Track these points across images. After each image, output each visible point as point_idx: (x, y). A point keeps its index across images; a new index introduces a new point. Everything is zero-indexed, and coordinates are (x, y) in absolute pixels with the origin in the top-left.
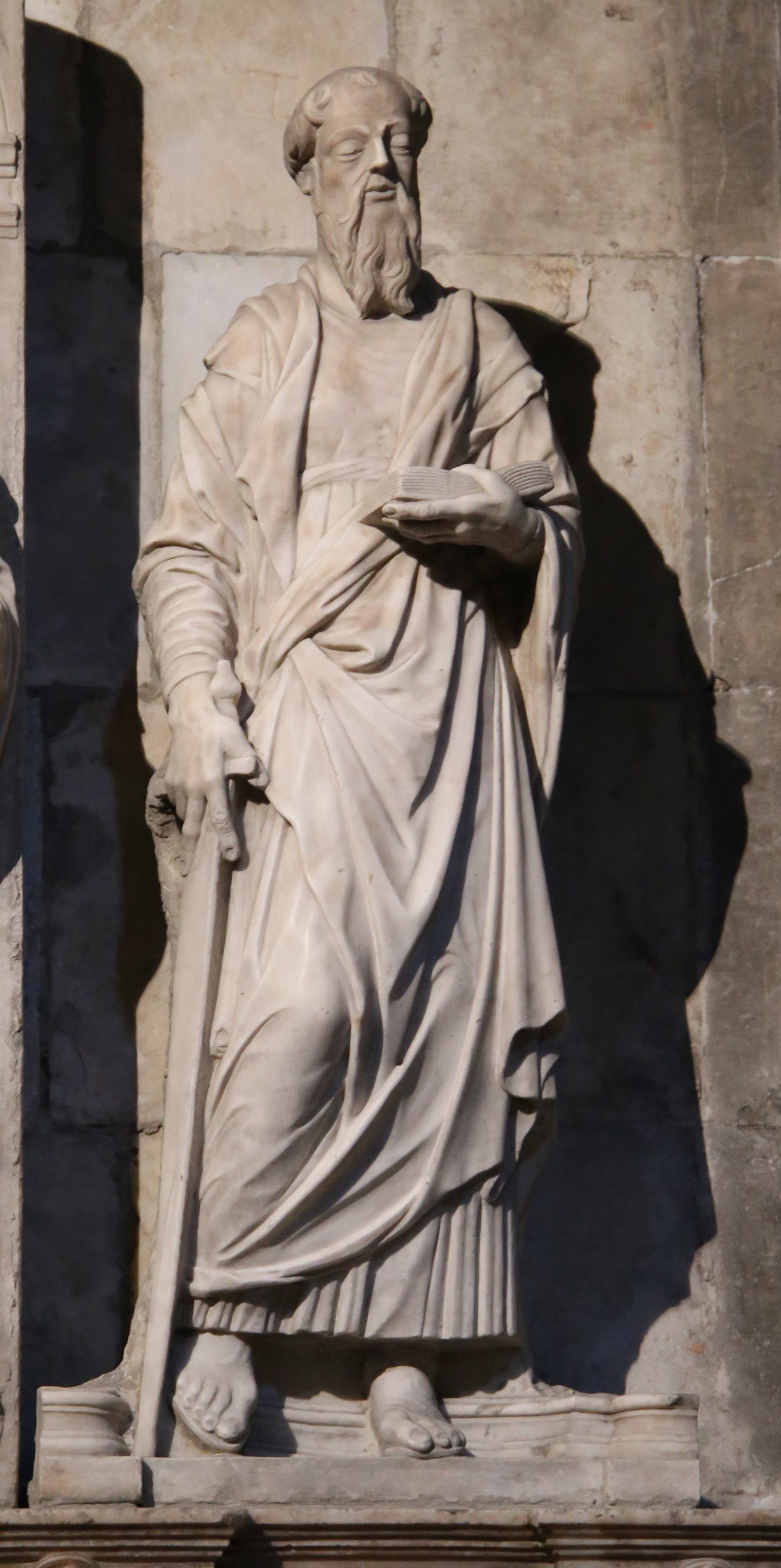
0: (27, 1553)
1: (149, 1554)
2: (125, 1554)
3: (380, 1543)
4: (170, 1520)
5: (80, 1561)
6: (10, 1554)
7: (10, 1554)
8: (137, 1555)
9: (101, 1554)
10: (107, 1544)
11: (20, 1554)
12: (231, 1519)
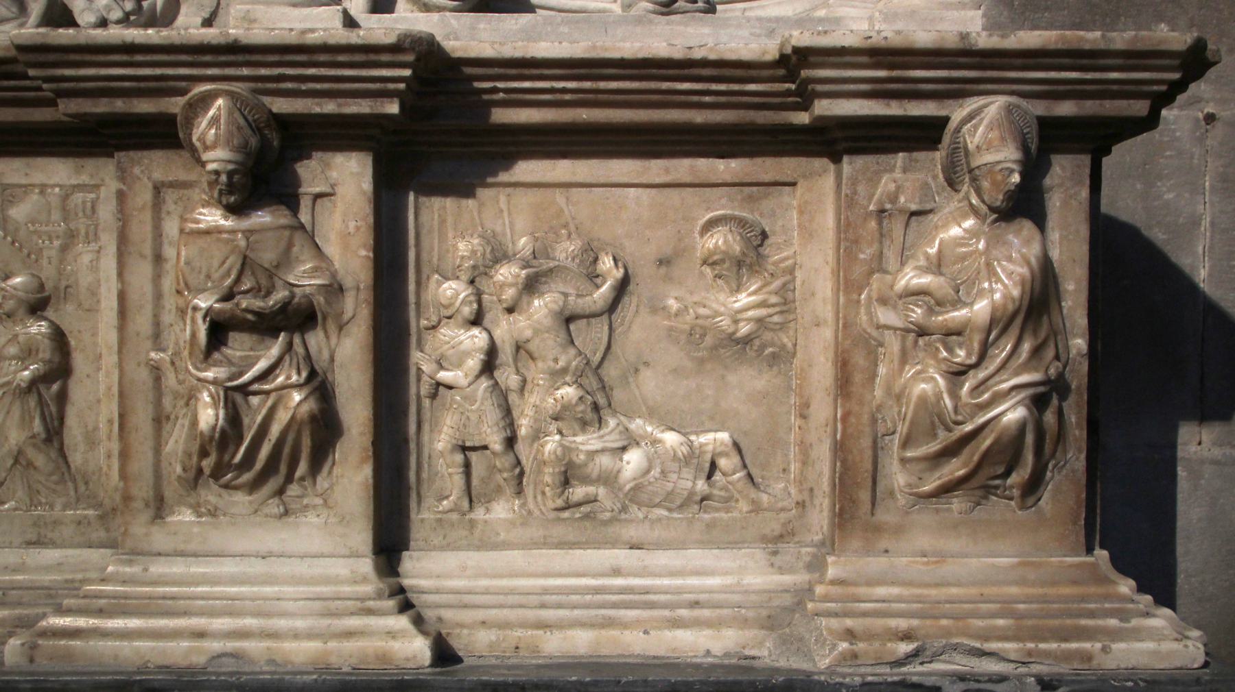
1: (318, 86)
2: (289, 85)
3: (602, 85)
5: (236, 93)
8: (304, 87)
12: (408, 40)
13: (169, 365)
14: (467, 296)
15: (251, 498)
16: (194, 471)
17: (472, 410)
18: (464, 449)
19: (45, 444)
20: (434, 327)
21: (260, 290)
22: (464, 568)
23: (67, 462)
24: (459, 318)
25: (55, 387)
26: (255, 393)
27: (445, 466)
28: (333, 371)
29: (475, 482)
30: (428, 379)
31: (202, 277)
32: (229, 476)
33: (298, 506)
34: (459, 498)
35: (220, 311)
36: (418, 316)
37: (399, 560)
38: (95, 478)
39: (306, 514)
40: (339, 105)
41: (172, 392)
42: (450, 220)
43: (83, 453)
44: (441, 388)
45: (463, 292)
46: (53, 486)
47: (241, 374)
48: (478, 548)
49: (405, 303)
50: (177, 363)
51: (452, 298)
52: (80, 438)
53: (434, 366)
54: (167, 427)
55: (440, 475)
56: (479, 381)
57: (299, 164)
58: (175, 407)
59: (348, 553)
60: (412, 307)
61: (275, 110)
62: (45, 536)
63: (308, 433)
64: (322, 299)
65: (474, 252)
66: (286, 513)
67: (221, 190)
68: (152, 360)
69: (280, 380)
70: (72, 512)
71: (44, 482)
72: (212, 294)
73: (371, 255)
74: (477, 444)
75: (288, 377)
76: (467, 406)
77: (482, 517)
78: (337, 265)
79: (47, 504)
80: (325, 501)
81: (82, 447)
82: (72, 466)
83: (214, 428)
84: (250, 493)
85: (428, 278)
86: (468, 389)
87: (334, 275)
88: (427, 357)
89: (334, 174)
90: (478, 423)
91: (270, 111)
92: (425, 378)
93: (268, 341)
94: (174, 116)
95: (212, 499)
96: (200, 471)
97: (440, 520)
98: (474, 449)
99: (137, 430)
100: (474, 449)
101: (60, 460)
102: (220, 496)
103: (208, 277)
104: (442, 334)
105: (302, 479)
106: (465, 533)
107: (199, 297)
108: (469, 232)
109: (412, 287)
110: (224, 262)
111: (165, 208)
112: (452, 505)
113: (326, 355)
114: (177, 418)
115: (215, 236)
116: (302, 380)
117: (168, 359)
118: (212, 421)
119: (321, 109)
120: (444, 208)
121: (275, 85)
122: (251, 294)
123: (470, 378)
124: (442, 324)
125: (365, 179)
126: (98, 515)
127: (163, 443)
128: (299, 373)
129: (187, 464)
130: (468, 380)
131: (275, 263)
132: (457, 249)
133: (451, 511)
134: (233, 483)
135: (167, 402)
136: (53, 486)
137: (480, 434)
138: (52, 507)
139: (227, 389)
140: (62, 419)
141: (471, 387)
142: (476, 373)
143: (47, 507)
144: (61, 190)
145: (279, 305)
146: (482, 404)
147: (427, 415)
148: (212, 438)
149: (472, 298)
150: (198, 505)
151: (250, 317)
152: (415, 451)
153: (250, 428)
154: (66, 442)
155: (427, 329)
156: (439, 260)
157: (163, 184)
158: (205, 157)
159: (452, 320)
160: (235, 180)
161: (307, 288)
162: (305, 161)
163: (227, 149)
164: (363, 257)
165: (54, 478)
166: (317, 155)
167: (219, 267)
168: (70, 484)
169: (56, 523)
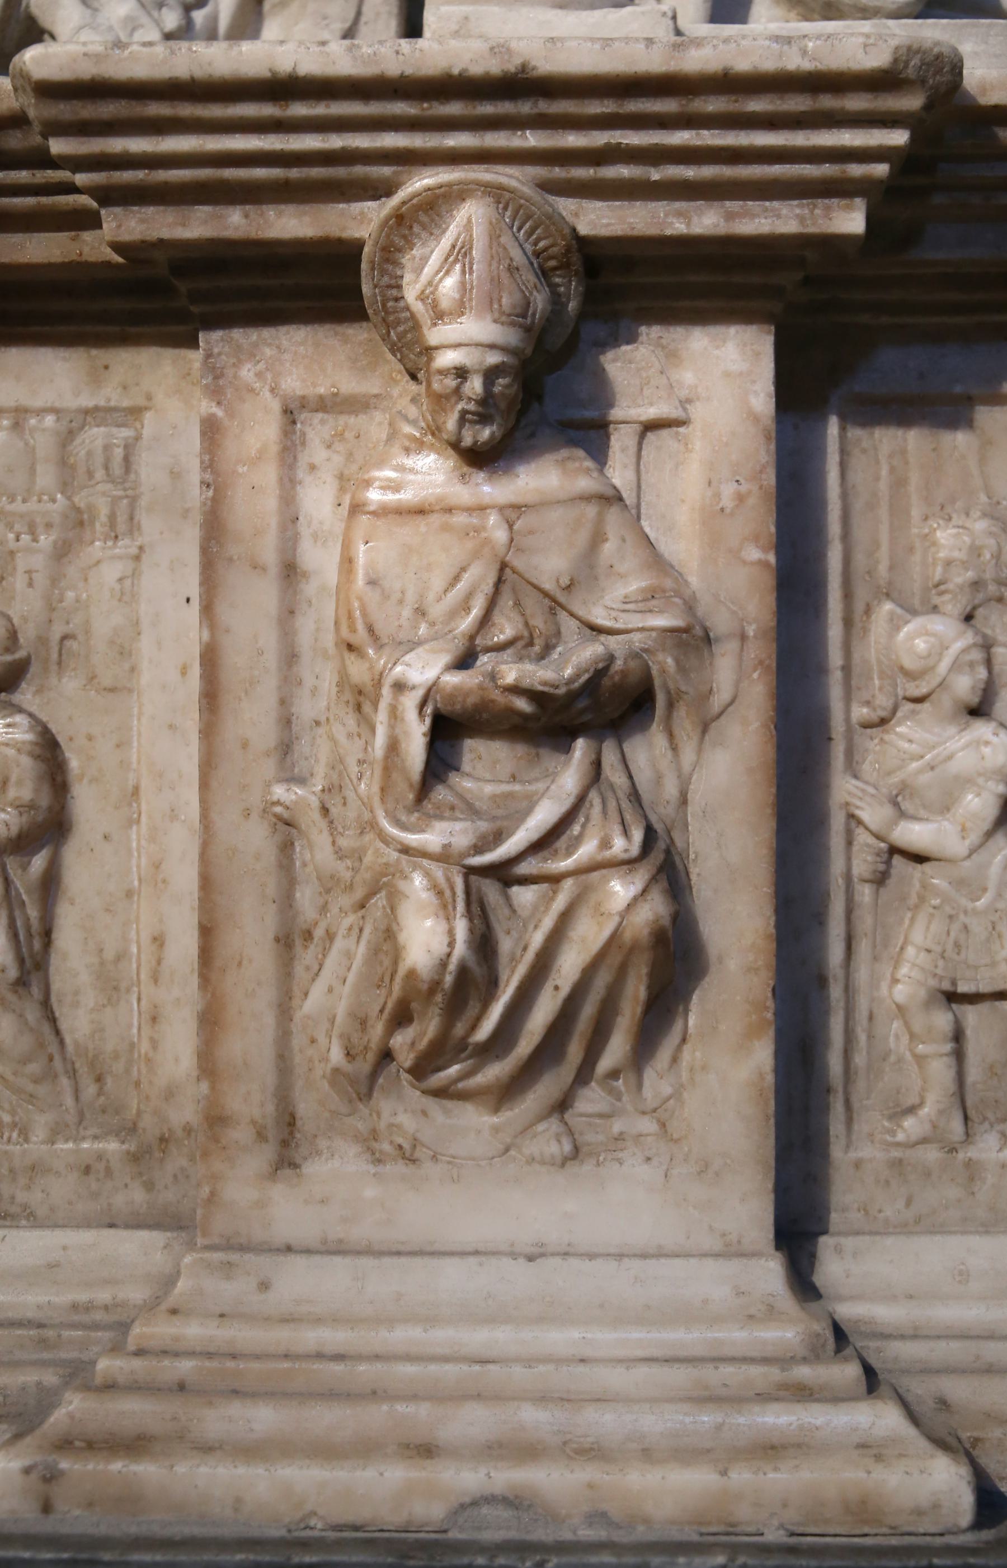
0: (360, 170)
1: (689, 172)
2: (624, 171)
4: (743, 65)
5: (501, 188)
6: (317, 172)
7: (317, 172)
8: (655, 175)
9: (558, 172)
10: (573, 140)
11: (340, 172)
12: (915, 62)
13: (316, 815)
14: (965, 651)
15: (495, 1120)
16: (371, 1057)
17: (974, 910)
18: (953, 997)
19: (16, 992)
20: (883, 722)
21: (531, 644)
22: (963, 1276)
23: (57, 1032)
24: (946, 702)
25: (39, 862)
26: (525, 881)
27: (905, 1039)
28: (686, 825)
29: (974, 1074)
30: (871, 840)
31: (407, 612)
32: (454, 1070)
33: (601, 1138)
34: (941, 1112)
35: (457, 692)
36: (848, 699)
37: (813, 1256)
38: (119, 1067)
39: (620, 1155)
40: (730, 217)
41: (319, 878)
42: (915, 479)
43: (92, 1010)
44: (897, 860)
45: (955, 640)
46: (30, 1087)
47: (498, 837)
48: (987, 1228)
49: (822, 669)
50: (334, 811)
51: (929, 655)
52: (85, 978)
53: (888, 811)
54: (306, 957)
55: (893, 1058)
56: (991, 843)
57: (610, 355)
58: (324, 909)
59: (718, 1246)
60: (835, 679)
61: (583, 230)
62: (13, 1198)
63: (644, 970)
64: (670, 661)
65: (976, 551)
66: (576, 1153)
67: (464, 413)
68: (278, 803)
69: (587, 850)
70: (70, 1145)
71: (11, 1078)
72: (433, 651)
73: (772, 558)
74: (984, 988)
75: (605, 844)
76: (964, 902)
77: (993, 1155)
78: (694, 581)
79: (14, 1125)
80: (663, 1125)
81: (90, 998)
82: (68, 1040)
83: (443, 964)
84: (496, 1110)
85: (868, 611)
86: (967, 864)
87: (690, 606)
88: (871, 790)
89: (687, 376)
90: (988, 940)
91: (574, 230)
92: (862, 837)
93: (550, 759)
94: (356, 247)
95: (407, 1121)
96: (386, 1056)
97: (899, 1163)
98: (974, 998)
99: (240, 964)
100: (974, 998)
101: (46, 1028)
102: (424, 1113)
103: (421, 612)
104: (900, 736)
105: (614, 1074)
106: (953, 1192)
107: (407, 658)
108: (959, 504)
109: (835, 632)
110: (457, 579)
111: (304, 459)
112: (927, 1127)
113: (671, 789)
114: (330, 936)
115: (436, 520)
116: (635, 850)
117: (314, 802)
118: (439, 945)
119: (688, 225)
120: (903, 452)
121: (592, 171)
122: (509, 651)
123: (974, 837)
124: (899, 714)
125: (757, 387)
126: (128, 1153)
127: (297, 992)
128: (626, 833)
129: (355, 1038)
130: (967, 842)
131: (565, 581)
132: (934, 544)
133: (924, 1141)
134: (460, 1085)
135: (306, 898)
136: (30, 1087)
137: (993, 964)
138: (25, 1134)
139: (470, 871)
140: (47, 935)
141: (974, 856)
142: (987, 825)
143: (15, 1135)
144: (58, 420)
145: (586, 676)
146: (999, 895)
147: (865, 921)
148: (435, 985)
149: (977, 655)
150: (374, 1134)
151: (522, 704)
152: (842, 1004)
153: (514, 961)
154: (55, 986)
155: (867, 725)
156: (891, 568)
157: (303, 403)
158: (434, 336)
159: (926, 706)
160: (497, 389)
161: (636, 637)
162: (625, 348)
163: (489, 318)
164: (752, 563)
165: (34, 1068)
166: (650, 333)
167: (446, 591)
168: (65, 1082)
169: (35, 1169)
